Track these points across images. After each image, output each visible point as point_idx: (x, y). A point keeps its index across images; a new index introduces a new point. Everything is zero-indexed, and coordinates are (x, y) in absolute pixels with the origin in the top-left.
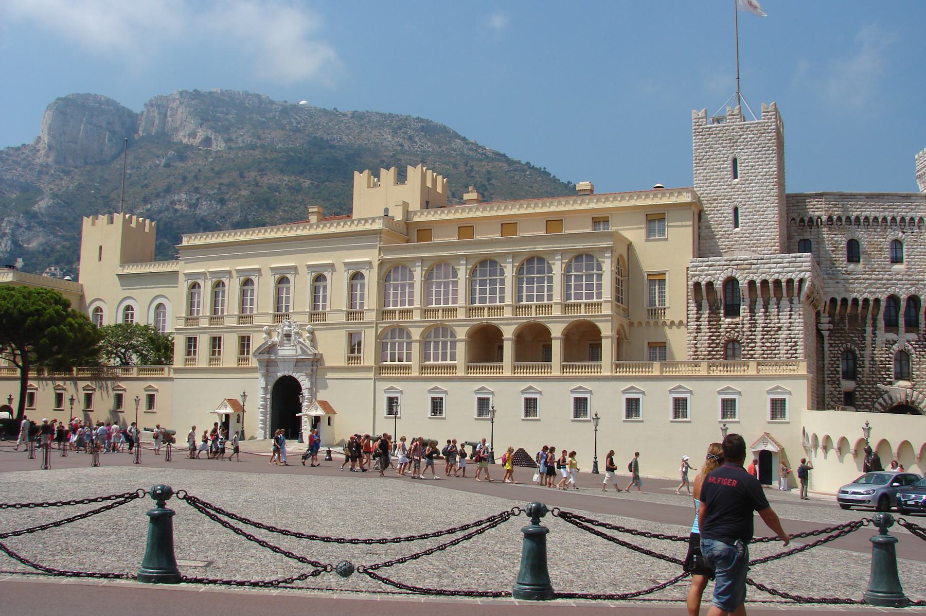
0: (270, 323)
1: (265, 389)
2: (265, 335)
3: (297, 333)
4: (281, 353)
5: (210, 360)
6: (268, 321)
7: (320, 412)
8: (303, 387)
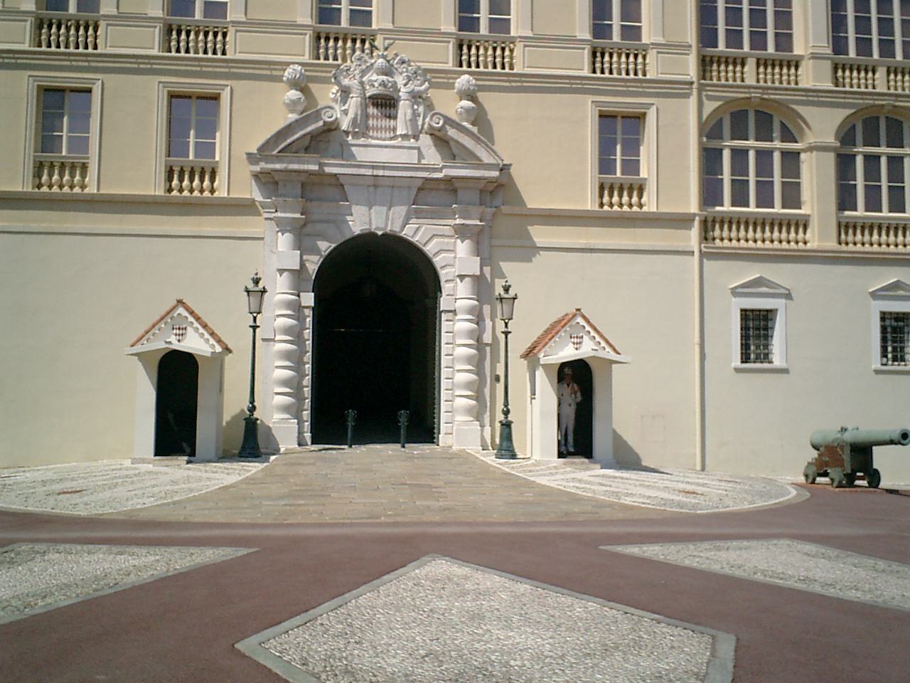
0: (306, 58)
1: (298, 275)
2: (294, 94)
3: (416, 97)
4: (362, 155)
5: (39, 168)
6: (296, 52)
7: (586, 350)
8: (443, 274)
